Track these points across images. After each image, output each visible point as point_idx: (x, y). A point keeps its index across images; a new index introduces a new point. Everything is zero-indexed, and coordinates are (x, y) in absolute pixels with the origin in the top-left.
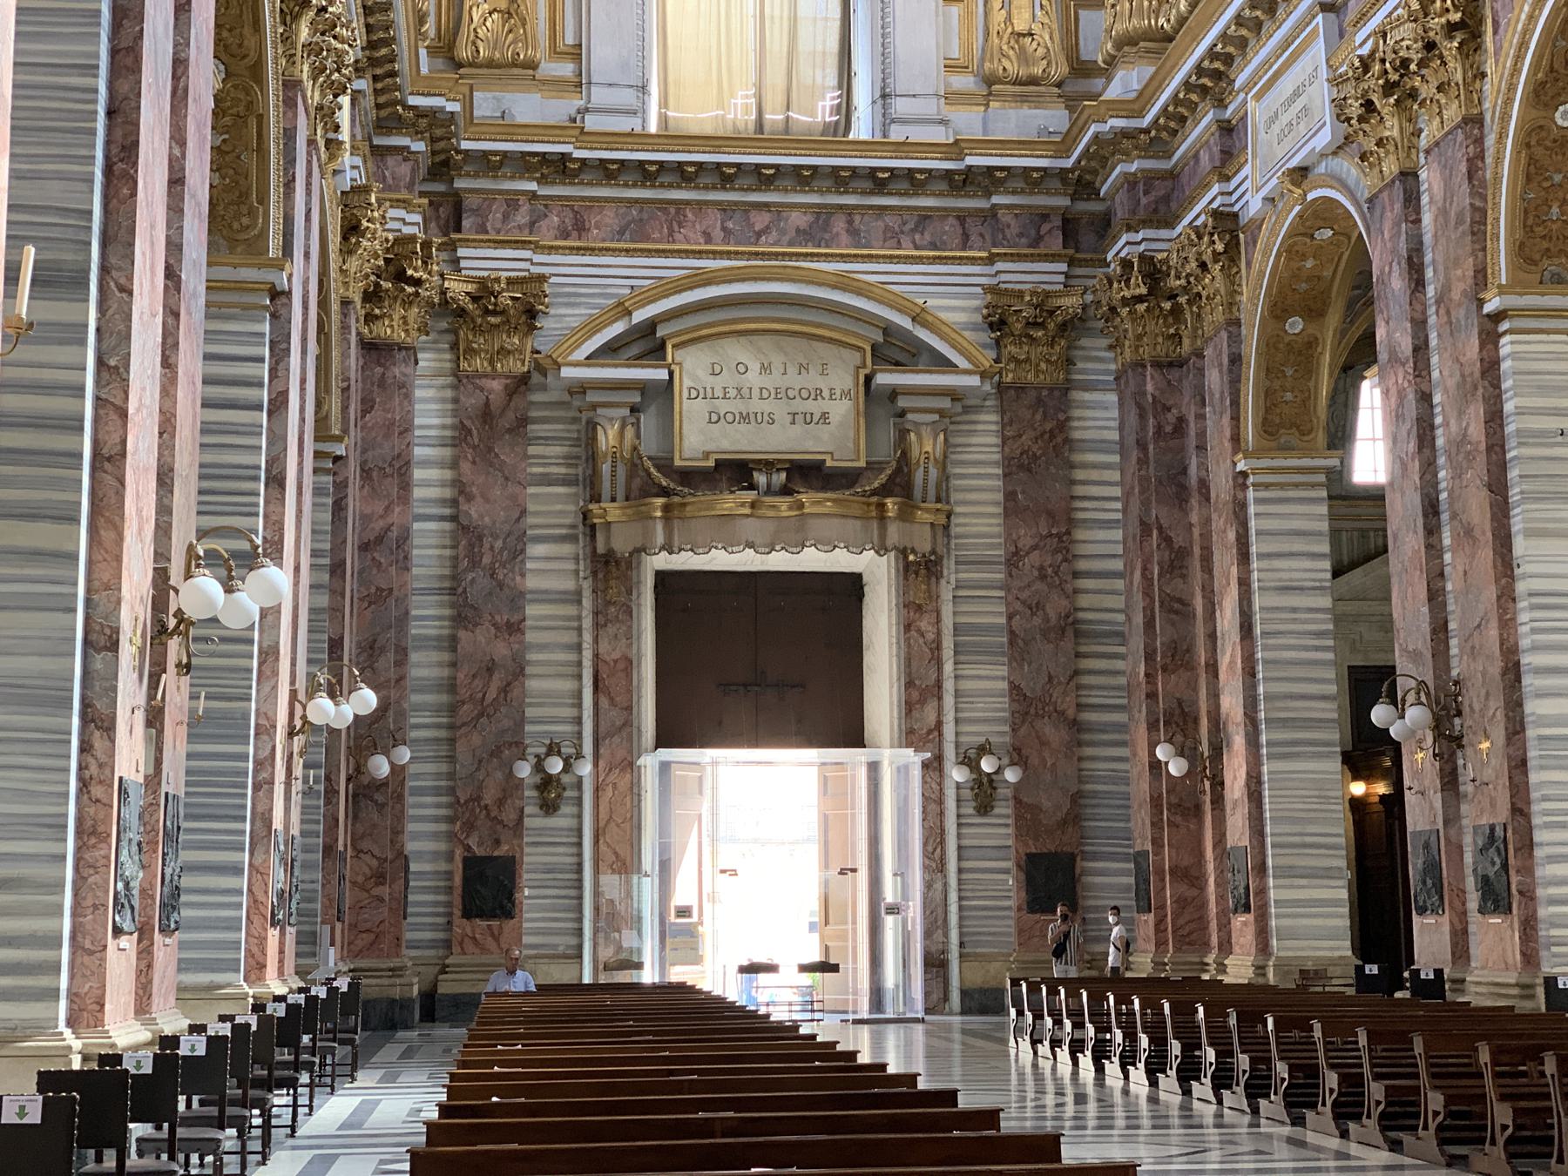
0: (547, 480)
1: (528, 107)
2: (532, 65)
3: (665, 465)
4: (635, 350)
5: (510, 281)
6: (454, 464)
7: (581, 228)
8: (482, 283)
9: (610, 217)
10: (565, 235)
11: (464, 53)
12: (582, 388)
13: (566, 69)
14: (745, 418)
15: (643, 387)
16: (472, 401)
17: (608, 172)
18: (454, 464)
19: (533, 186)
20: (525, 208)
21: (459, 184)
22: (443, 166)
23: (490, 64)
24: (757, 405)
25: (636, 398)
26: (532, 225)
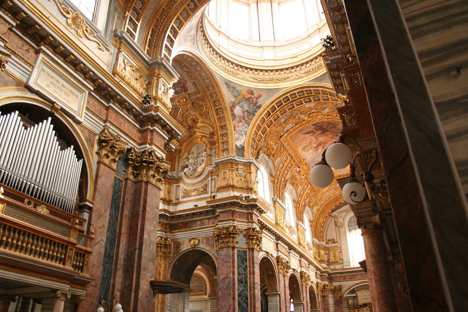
0: (345, 308)
1: (338, 267)
2: (337, 262)
3: (357, 305)
4: (352, 292)
5: (338, 286)
6: (335, 307)
7: (345, 279)
8: (335, 286)
9: (348, 277)
10: (343, 280)
11: (330, 262)
12: (347, 297)
13: (341, 261)
14: (366, 298)
15: (354, 296)
16: (336, 300)
17: (348, 272)
18: (335, 307)
19: (339, 275)
20: (339, 277)
21: (332, 276)
22: (329, 274)
23: (333, 262)
24: (367, 297)
25: (353, 298)
26: (340, 279)
